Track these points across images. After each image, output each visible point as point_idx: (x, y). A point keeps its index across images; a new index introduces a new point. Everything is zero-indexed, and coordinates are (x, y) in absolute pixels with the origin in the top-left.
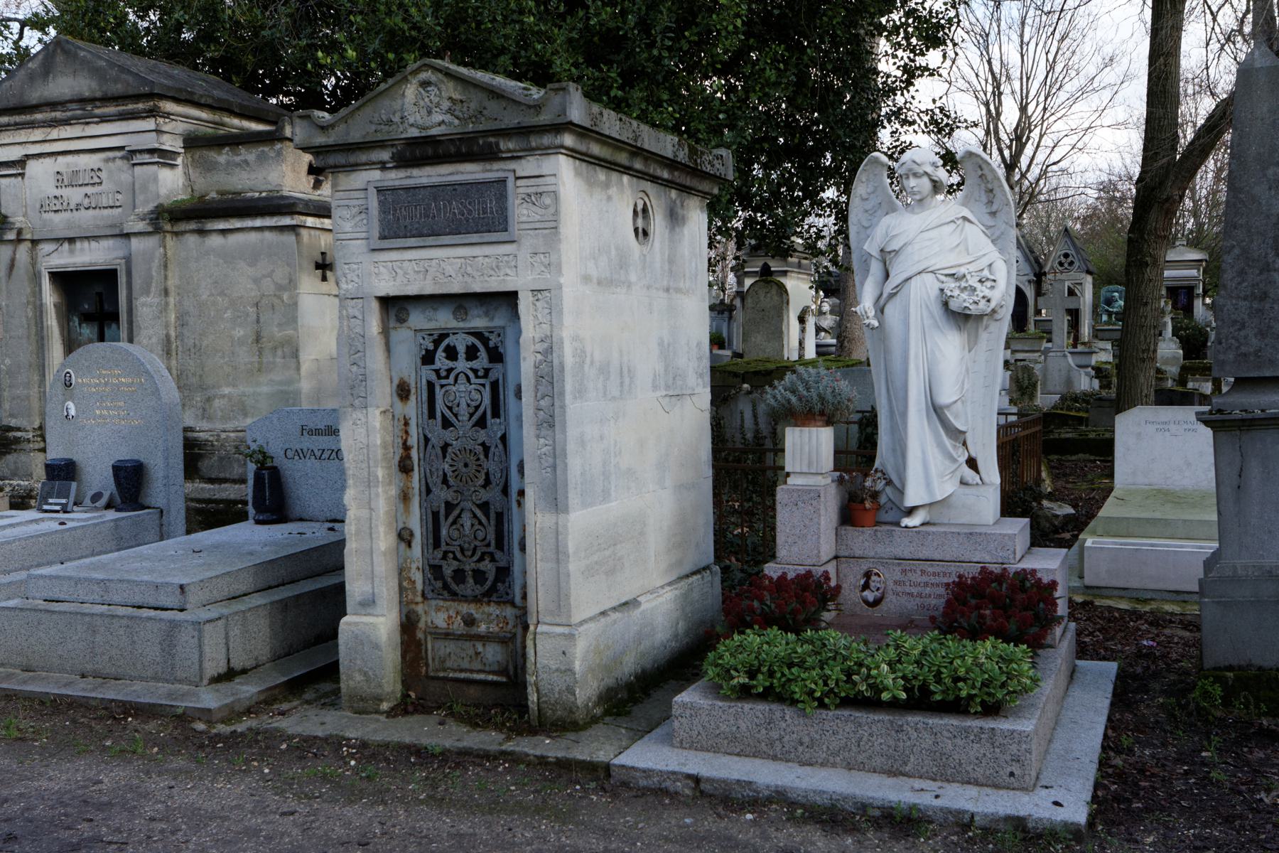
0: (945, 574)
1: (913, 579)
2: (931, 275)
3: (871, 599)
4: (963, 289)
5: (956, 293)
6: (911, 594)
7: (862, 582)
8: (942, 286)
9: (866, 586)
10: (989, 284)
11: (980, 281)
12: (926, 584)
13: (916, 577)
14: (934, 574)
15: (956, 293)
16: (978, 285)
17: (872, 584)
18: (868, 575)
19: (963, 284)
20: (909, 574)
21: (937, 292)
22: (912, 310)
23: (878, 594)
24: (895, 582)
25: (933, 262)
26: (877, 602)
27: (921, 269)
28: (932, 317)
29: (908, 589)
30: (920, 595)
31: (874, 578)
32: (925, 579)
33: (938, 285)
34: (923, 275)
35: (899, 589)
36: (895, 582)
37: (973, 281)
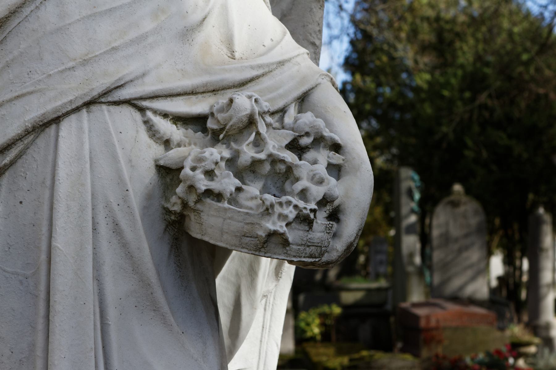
2: (127, 111)
4: (247, 172)
5: (227, 182)
8: (172, 156)
10: (323, 157)
11: (294, 146)
15: (227, 182)
16: (290, 157)
19: (248, 153)
21: (148, 175)
22: (63, 241)
25: (131, 68)
27: (99, 85)
28: (135, 268)
33: (149, 152)
34: (104, 112)
37: (275, 144)
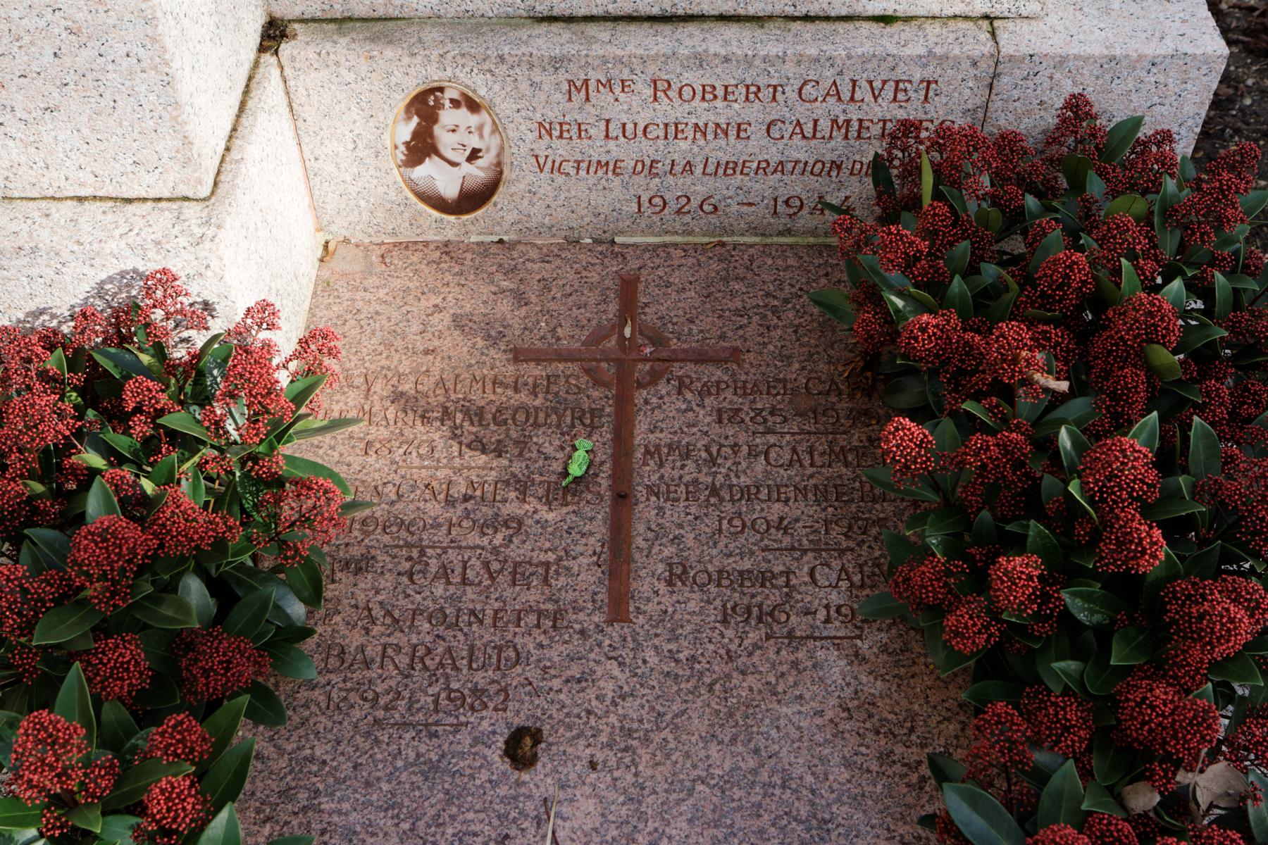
0: (752, 92)
1: (618, 113)
3: (450, 191)
6: (615, 168)
7: (406, 131)
9: (422, 147)
12: (674, 130)
13: (634, 107)
14: (708, 93)
17: (444, 140)
18: (424, 106)
20: (602, 98)
23: (477, 173)
24: (545, 129)
26: (473, 200)
29: (596, 149)
30: (651, 168)
31: (448, 116)
32: (669, 110)
35: (561, 149)
36: (545, 129)
